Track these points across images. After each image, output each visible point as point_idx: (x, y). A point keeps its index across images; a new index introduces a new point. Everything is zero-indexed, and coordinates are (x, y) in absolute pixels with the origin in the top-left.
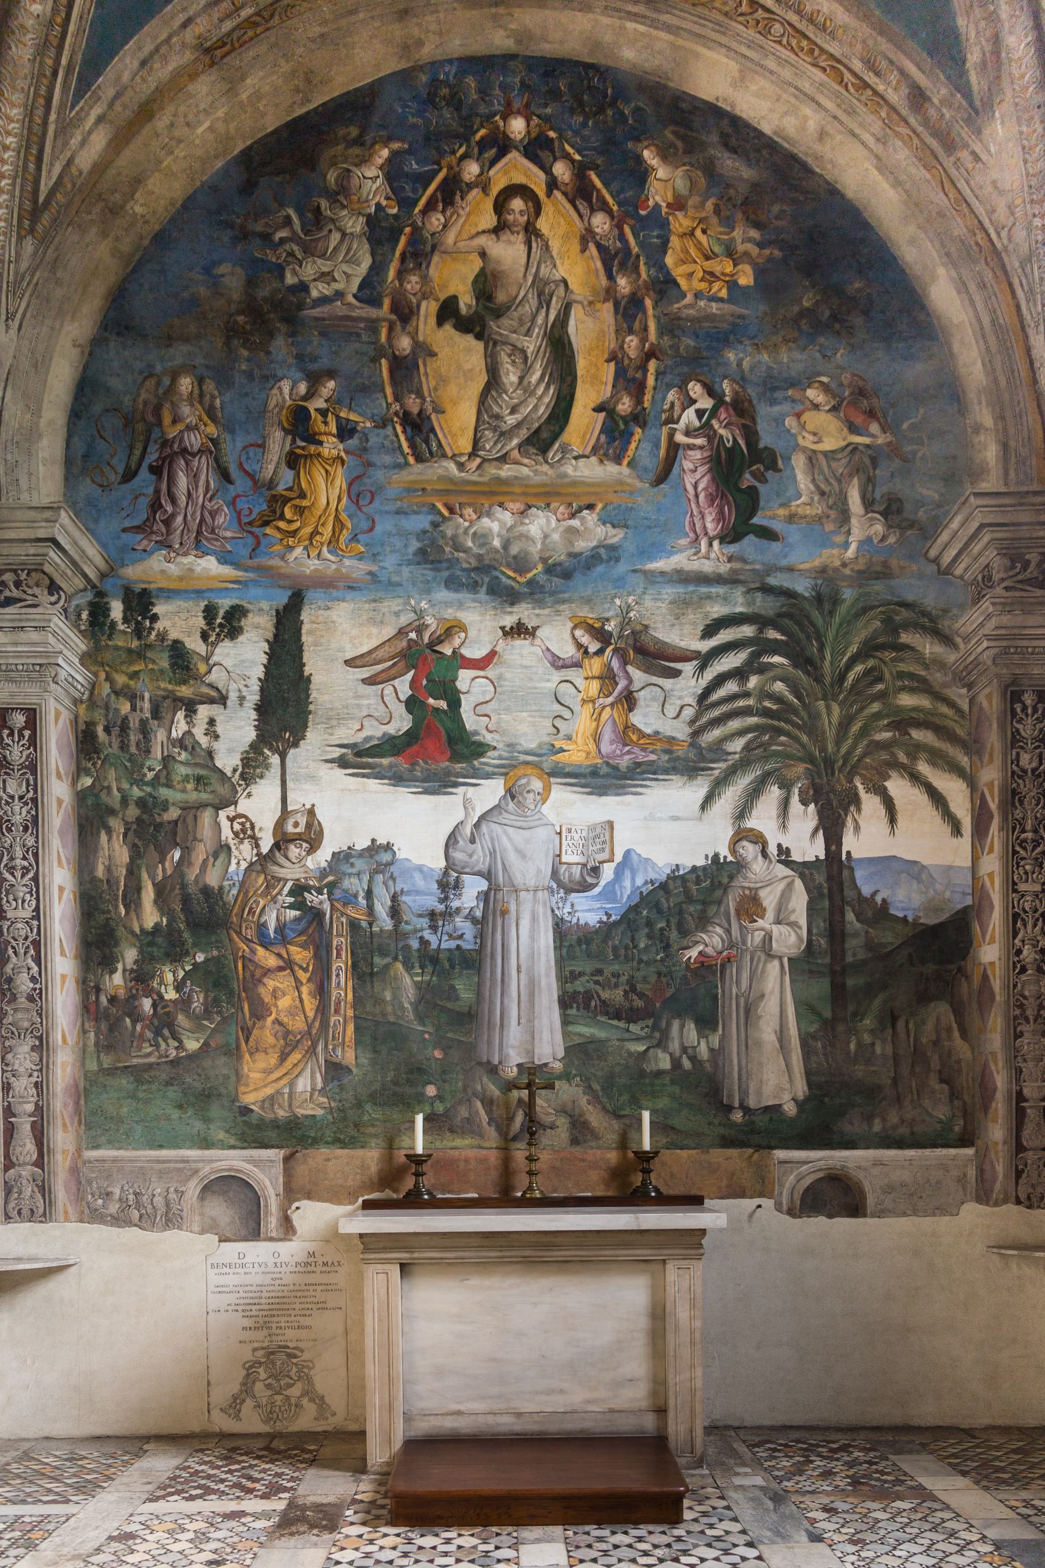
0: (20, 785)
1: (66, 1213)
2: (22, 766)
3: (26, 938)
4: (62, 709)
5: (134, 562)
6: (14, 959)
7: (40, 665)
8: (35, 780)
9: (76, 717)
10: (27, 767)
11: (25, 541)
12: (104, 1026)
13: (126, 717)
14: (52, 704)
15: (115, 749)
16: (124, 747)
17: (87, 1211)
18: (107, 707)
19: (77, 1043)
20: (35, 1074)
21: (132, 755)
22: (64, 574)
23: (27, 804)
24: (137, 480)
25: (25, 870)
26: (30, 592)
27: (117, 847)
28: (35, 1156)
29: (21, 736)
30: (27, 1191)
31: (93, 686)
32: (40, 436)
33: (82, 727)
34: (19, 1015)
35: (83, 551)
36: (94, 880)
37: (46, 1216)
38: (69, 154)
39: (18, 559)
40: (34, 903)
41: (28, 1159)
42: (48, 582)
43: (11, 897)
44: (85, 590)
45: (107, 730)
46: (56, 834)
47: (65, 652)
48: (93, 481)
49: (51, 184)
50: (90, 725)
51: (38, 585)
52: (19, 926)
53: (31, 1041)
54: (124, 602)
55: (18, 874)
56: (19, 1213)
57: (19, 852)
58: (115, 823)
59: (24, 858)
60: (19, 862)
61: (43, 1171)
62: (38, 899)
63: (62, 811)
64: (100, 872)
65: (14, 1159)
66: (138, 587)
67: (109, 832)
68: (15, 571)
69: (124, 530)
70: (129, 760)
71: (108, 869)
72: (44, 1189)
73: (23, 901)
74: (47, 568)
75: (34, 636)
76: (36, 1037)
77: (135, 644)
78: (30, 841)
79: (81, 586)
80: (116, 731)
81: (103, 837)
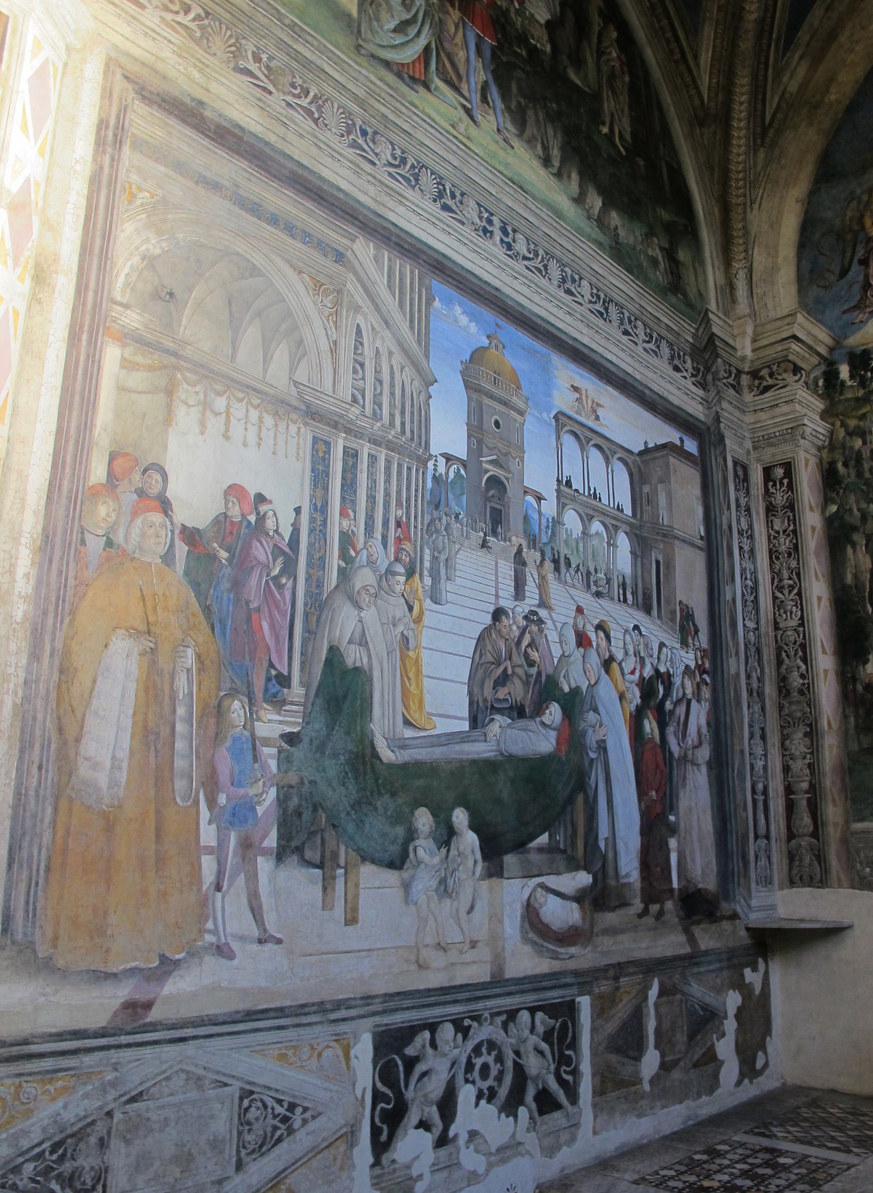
0: (783, 522)
1: (839, 879)
2: (784, 507)
3: (795, 643)
4: (809, 457)
5: (853, 333)
6: (787, 661)
7: (792, 428)
8: (794, 516)
9: (821, 460)
10: (787, 507)
11: (773, 344)
12: (861, 711)
13: (859, 451)
14: (802, 455)
15: (853, 478)
16: (860, 475)
17: (857, 879)
18: (843, 447)
19: (840, 728)
20: (808, 756)
21: (867, 480)
22: (803, 358)
23: (788, 535)
24: (851, 273)
25: (791, 587)
26: (780, 377)
27: (861, 556)
28: (811, 829)
29: (782, 484)
30: (807, 859)
31: (832, 433)
32: (779, 269)
33: (826, 466)
34: (794, 707)
35: (815, 337)
36: (845, 587)
37: (823, 882)
38: (782, 88)
39: (770, 358)
40: (799, 613)
41: (805, 831)
42: (792, 366)
43: (782, 611)
44: (820, 364)
45: (845, 465)
46: (813, 556)
47: (809, 414)
48: (818, 286)
49: (772, 111)
50: (832, 464)
51: (785, 371)
52: (789, 633)
53: (803, 729)
54: (849, 364)
55: (786, 592)
56: (801, 879)
57: (786, 575)
58: (859, 538)
59: (790, 578)
60: (787, 582)
61: (818, 840)
62: (802, 610)
63: (816, 536)
64: (849, 579)
65: (795, 831)
66: (858, 351)
67: (854, 545)
68: (769, 367)
69: (844, 312)
70: (865, 484)
71: (856, 576)
72: (820, 857)
73: (791, 613)
74: (791, 357)
75: (785, 408)
76: (807, 725)
77: (861, 393)
78: (794, 564)
79: (817, 362)
80: (852, 463)
81: (849, 550)
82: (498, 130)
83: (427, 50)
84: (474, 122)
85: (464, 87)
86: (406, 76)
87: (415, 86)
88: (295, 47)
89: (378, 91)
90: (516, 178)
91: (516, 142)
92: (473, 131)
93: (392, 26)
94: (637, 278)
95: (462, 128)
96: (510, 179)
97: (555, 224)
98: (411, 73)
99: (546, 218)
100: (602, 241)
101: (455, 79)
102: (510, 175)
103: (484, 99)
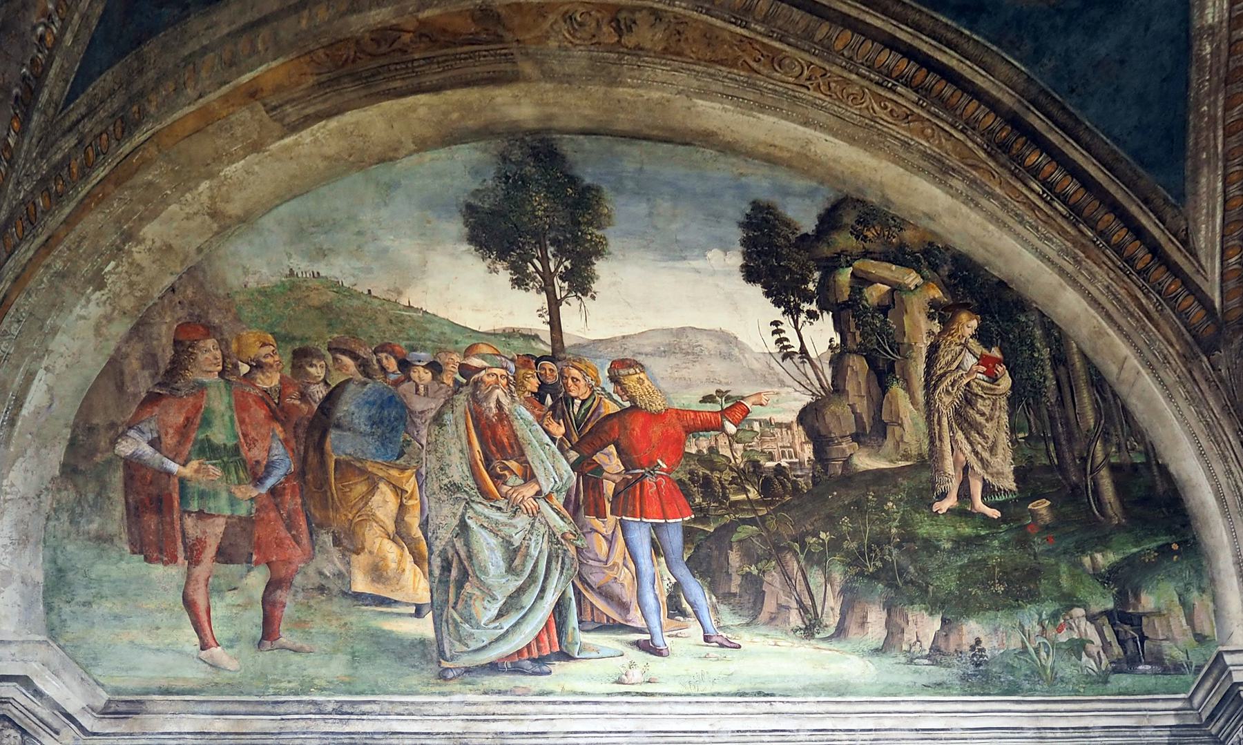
82: (707, 639)
83: (560, 609)
84: (657, 652)
85: (636, 618)
86: (527, 665)
87: (545, 668)
88: (347, 729)
89: (482, 709)
90: (747, 687)
91: (745, 638)
92: (657, 666)
93: (494, 610)
94: (1031, 691)
95: (636, 675)
96: (736, 694)
97: (833, 708)
98: (535, 654)
99: (814, 708)
100: (939, 679)
101: (615, 615)
102: (734, 689)
103: (675, 607)
